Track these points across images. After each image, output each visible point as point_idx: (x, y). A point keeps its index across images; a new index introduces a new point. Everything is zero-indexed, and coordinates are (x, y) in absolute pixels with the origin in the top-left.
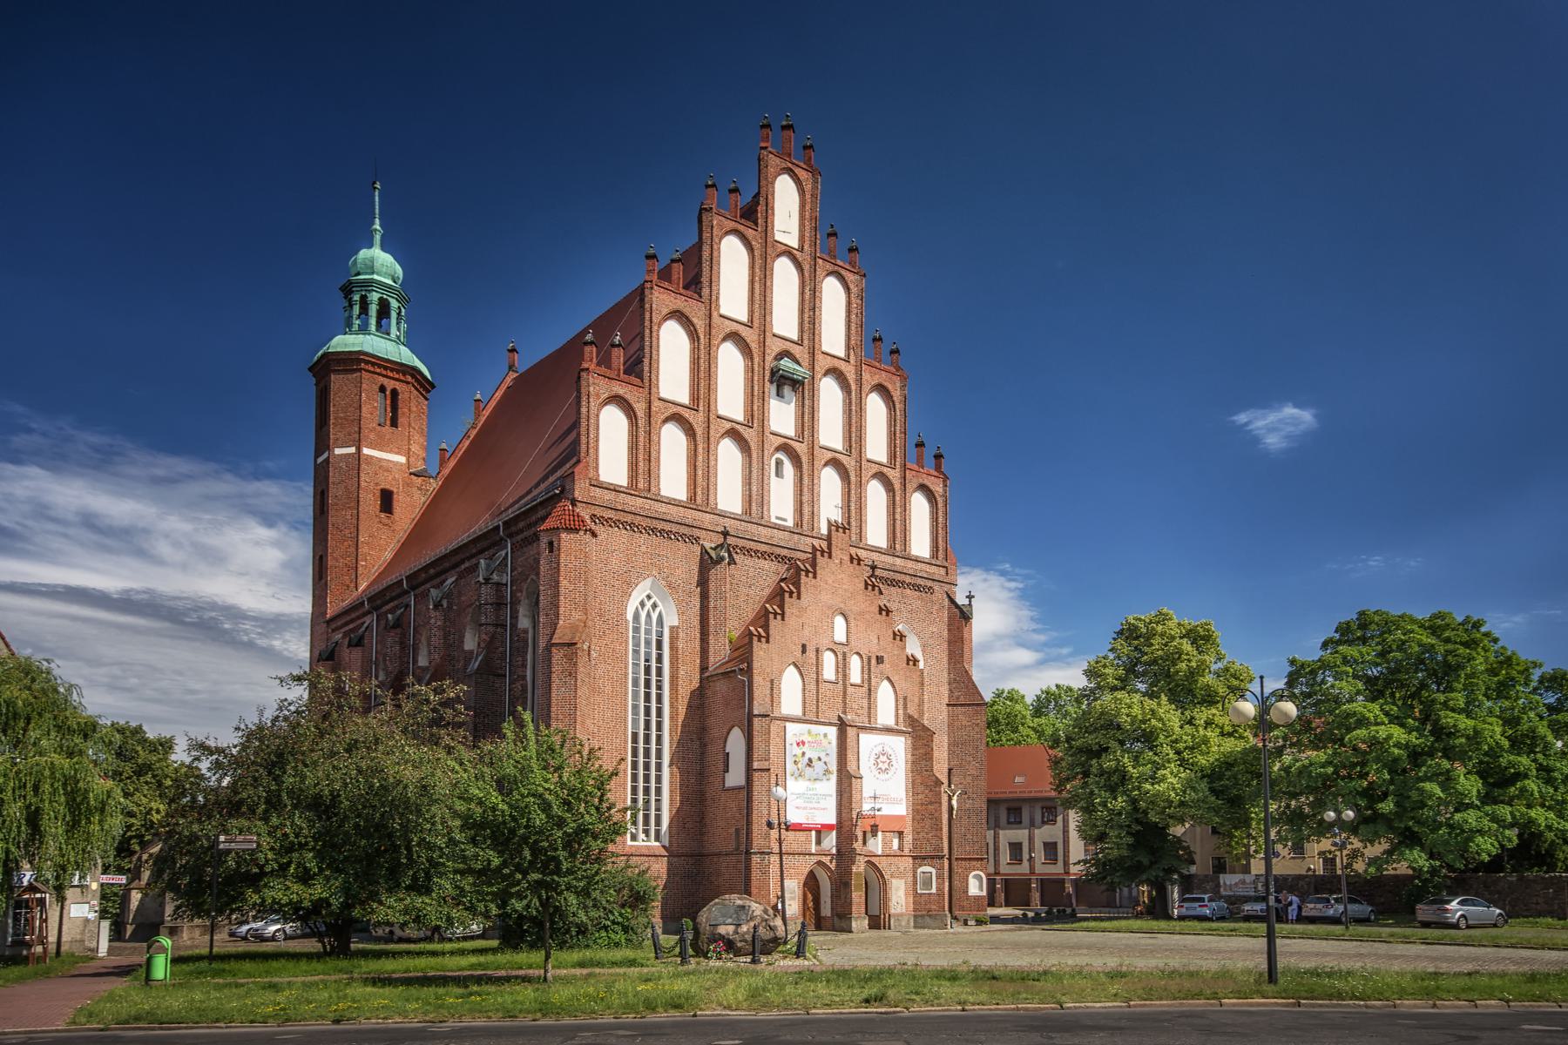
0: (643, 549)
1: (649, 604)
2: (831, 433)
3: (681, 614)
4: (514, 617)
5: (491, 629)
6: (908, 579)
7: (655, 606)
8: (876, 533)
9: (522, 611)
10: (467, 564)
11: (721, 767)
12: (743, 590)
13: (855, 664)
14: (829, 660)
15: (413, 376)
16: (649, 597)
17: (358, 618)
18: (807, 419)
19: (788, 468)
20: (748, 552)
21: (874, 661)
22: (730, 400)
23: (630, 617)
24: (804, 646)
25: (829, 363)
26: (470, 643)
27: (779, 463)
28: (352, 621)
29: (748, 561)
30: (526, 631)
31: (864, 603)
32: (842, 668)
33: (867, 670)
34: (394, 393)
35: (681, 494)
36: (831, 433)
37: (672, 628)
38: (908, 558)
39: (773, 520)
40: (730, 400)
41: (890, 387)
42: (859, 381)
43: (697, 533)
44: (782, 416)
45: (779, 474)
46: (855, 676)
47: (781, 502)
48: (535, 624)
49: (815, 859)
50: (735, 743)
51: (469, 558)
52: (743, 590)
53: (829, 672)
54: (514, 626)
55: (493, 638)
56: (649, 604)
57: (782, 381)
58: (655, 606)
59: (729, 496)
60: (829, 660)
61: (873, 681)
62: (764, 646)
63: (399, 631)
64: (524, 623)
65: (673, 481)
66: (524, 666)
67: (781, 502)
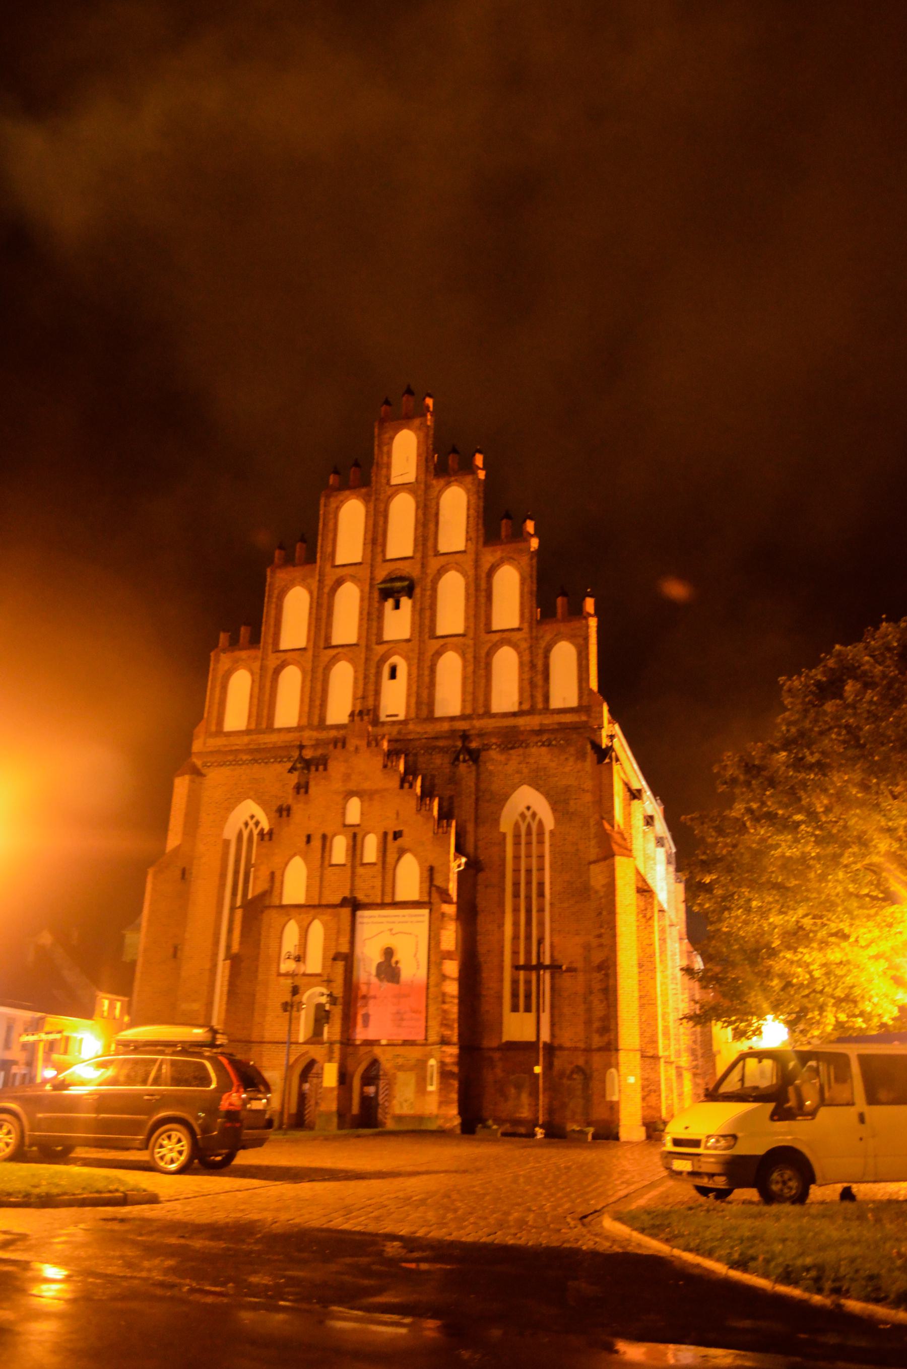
1: (251, 824)
21: (390, 837)
32: (355, 848)
45: (393, 676)
56: (251, 824)
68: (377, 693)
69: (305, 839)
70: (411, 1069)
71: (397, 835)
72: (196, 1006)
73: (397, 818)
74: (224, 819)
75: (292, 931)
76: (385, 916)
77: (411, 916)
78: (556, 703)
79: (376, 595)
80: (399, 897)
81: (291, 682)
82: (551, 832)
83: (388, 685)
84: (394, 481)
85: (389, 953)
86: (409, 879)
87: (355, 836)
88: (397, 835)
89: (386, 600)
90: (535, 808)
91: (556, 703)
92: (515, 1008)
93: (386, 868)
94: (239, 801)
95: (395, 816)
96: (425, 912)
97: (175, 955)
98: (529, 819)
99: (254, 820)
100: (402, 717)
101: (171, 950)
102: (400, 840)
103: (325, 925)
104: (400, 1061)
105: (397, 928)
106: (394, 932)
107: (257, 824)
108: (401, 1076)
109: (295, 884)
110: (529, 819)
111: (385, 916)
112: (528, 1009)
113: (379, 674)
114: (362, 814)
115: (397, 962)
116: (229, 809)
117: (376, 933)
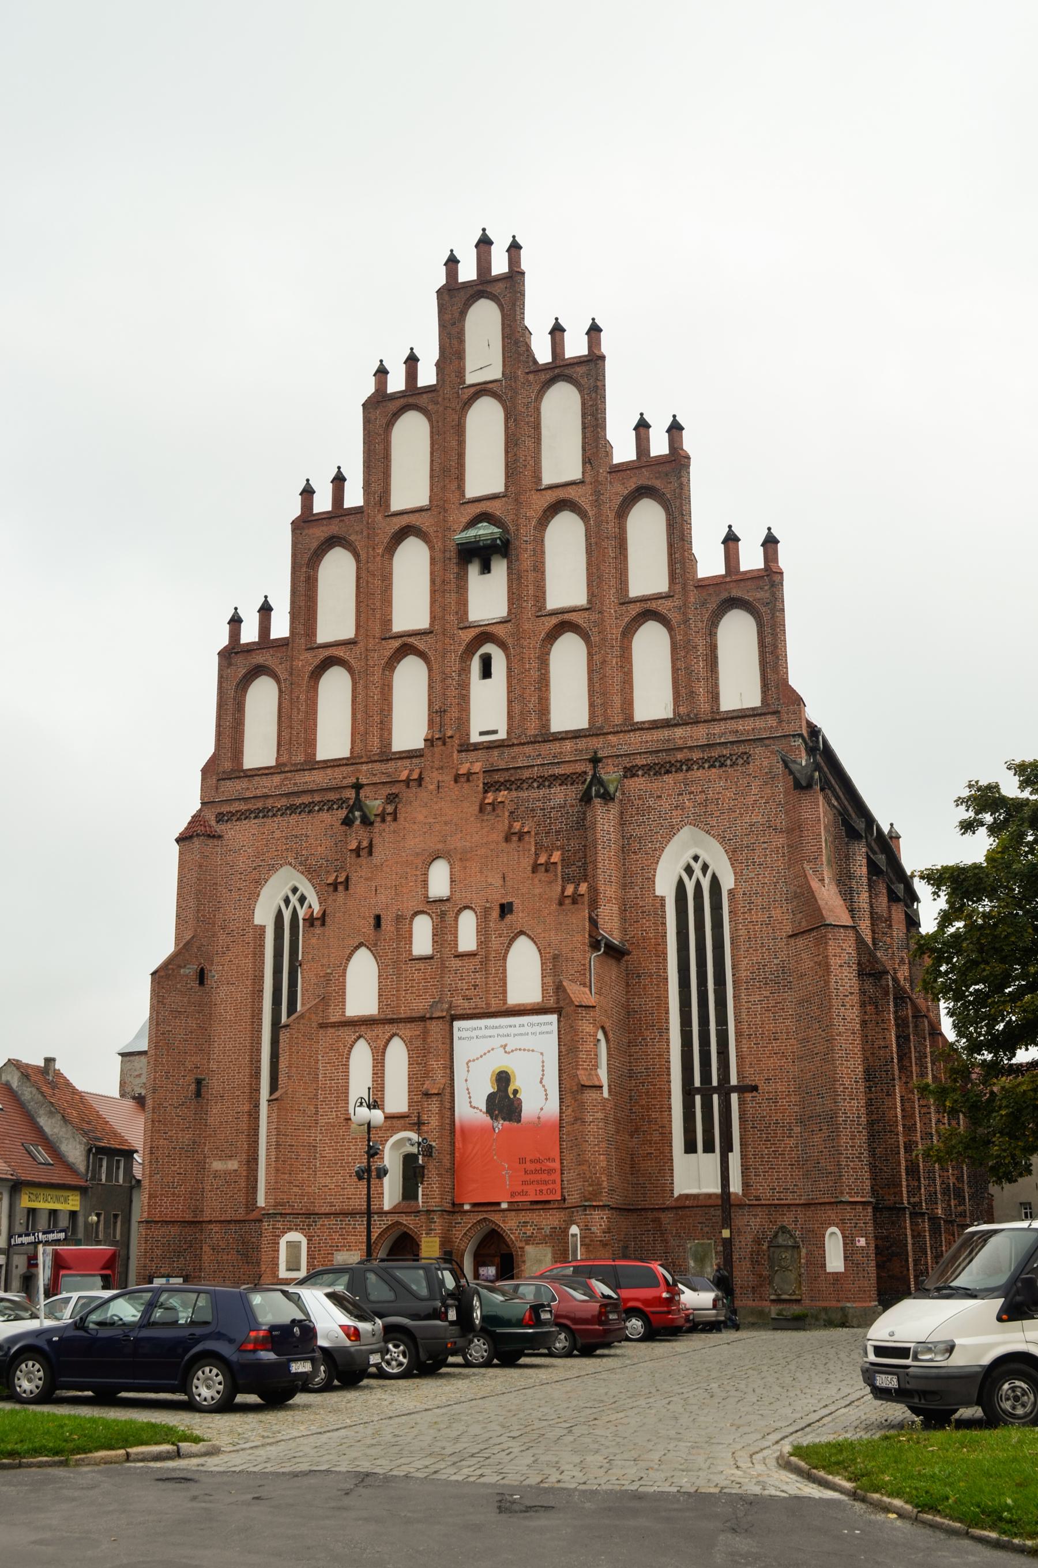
0: (277, 834)
1: (294, 900)
6: (696, 755)
16: (295, 890)
18: (527, 587)
21: (495, 913)
22: (411, 608)
24: (378, 919)
25: (550, 497)
32: (444, 933)
33: (483, 931)
38: (718, 717)
40: (411, 608)
41: (657, 484)
42: (597, 503)
44: (487, 597)
45: (486, 673)
49: (389, 1220)
56: (294, 900)
57: (480, 555)
61: (495, 943)
68: (464, 700)
69: (372, 921)
70: (544, 1241)
71: (505, 909)
72: (233, 1165)
73: (504, 886)
74: (254, 896)
75: (361, 1056)
76: (493, 1027)
77: (532, 1025)
78: (728, 703)
80: (515, 997)
82: (731, 892)
83: (478, 687)
84: (471, 379)
85: (503, 1079)
86: (524, 973)
87: (443, 915)
88: (505, 909)
89: (469, 562)
90: (704, 856)
91: (728, 703)
92: (690, 1147)
93: (490, 960)
94: (273, 869)
95: (501, 882)
96: (553, 1018)
97: (198, 1094)
98: (698, 872)
99: (298, 894)
100: (502, 735)
101: (193, 1087)
102: (509, 918)
103: (409, 1043)
104: (529, 1230)
105: (512, 1043)
106: (508, 1049)
107: (302, 899)
108: (530, 1249)
109: (362, 989)
110: (698, 872)
111: (493, 1027)
112: (709, 1148)
113: (465, 671)
115: (516, 1092)
116: (259, 882)
117: (481, 1052)
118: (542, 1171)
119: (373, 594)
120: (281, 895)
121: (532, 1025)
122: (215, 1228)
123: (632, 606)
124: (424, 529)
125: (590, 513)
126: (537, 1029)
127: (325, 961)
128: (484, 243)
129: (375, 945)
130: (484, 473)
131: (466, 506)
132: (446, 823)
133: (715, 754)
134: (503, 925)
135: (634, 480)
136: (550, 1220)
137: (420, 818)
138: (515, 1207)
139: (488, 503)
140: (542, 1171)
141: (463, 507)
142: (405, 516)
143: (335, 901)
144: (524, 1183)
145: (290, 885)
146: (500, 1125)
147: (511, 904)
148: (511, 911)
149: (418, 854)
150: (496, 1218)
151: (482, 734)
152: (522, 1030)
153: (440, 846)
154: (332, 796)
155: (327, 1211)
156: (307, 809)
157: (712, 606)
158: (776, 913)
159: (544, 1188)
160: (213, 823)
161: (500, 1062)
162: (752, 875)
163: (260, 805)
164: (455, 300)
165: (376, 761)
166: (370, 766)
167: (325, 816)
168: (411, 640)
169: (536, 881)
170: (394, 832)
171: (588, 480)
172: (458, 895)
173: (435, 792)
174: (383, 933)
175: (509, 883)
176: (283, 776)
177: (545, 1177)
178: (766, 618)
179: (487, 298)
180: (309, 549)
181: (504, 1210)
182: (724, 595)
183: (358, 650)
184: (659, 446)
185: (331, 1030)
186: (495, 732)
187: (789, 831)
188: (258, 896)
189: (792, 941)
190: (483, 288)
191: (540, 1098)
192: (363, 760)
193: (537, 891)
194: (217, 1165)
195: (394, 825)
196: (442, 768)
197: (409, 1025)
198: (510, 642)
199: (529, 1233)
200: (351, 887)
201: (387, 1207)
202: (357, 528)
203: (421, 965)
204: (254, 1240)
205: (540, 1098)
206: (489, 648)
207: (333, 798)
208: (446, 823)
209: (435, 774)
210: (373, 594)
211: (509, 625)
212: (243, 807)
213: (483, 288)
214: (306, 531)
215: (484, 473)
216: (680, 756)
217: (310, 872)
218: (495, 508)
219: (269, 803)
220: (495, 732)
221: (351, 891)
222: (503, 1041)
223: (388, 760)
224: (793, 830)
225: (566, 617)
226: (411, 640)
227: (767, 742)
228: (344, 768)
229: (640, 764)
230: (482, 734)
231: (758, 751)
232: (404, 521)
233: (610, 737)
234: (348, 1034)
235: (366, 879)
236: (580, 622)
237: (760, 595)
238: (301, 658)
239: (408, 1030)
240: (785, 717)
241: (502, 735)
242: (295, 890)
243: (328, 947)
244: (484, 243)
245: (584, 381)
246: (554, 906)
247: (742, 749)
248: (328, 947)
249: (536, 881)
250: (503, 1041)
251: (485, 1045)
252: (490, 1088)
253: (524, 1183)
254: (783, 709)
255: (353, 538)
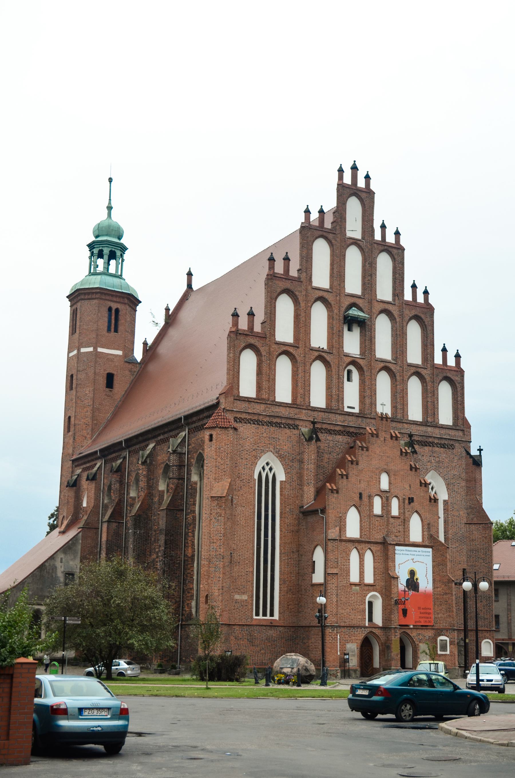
0: (265, 435)
1: (267, 468)
2: (383, 350)
3: (286, 473)
4: (189, 474)
5: (176, 481)
6: (436, 441)
7: (271, 469)
8: (415, 412)
9: (193, 470)
10: (162, 437)
11: (310, 570)
12: (326, 456)
13: (395, 504)
14: (377, 502)
15: (128, 299)
16: (268, 464)
17: (93, 460)
19: (355, 375)
20: (330, 432)
21: (407, 501)
22: (319, 338)
23: (256, 477)
24: (361, 494)
25: (382, 306)
26: (162, 487)
27: (349, 372)
28: (89, 462)
29: (330, 438)
30: (196, 483)
31: (401, 465)
32: (386, 506)
34: (117, 311)
35: (288, 399)
36: (383, 350)
37: (281, 482)
39: (346, 409)
40: (319, 338)
41: (423, 316)
42: (402, 315)
43: (297, 422)
44: (351, 343)
45: (349, 380)
46: (395, 511)
47: (351, 397)
48: (201, 477)
49: (368, 630)
50: (319, 556)
51: (164, 433)
52: (326, 456)
53: (377, 509)
54: (189, 479)
55: (177, 487)
56: (267, 468)
57: (351, 322)
58: (271, 469)
59: (318, 398)
60: (377, 502)
61: (407, 515)
62: (335, 495)
63: (119, 474)
64: (195, 478)
65: (283, 393)
66: (195, 504)
67: (351, 397)
71: (411, 500)
72: (245, 597)
75: (354, 556)
77: (423, 552)
79: (342, 318)
81: (284, 368)
83: (347, 385)
85: (412, 573)
88: (411, 500)
94: (263, 452)
96: (430, 550)
100: (357, 410)
105: (416, 558)
106: (414, 561)
114: (390, 483)
115: (417, 579)
116: (257, 458)
118: (426, 613)
119: (302, 323)
120: (262, 466)
121: (423, 552)
122: (237, 628)
123: (412, 368)
124: (329, 301)
125: (398, 320)
126: (424, 554)
127: (339, 510)
128: (354, 168)
129: (360, 506)
130: (353, 285)
131: (348, 297)
132: (388, 457)
133: (443, 442)
134: (410, 507)
135: (414, 311)
136: (429, 633)
137: (378, 452)
138: (416, 627)
139: (357, 299)
140: (426, 613)
141: (346, 297)
142: (321, 291)
143: (342, 483)
144: (420, 617)
145: (266, 462)
146: (411, 592)
147: (413, 498)
148: (413, 501)
149: (377, 468)
150: (408, 631)
151: (348, 407)
152: (419, 553)
153: (386, 467)
154: (291, 422)
155: (343, 625)
156: (278, 425)
157: (441, 378)
158: (461, 513)
159: (427, 620)
160: (233, 421)
161: (411, 566)
162: (454, 496)
163: (256, 418)
164: (345, 191)
165: (309, 410)
166: (306, 411)
167: (287, 431)
168: (323, 354)
169: (422, 490)
170: (367, 456)
171: (397, 304)
172: (392, 491)
173: (383, 442)
174: (362, 503)
175: (412, 489)
176: (266, 405)
177: (427, 616)
178: (459, 389)
179: (357, 197)
180: (276, 291)
181: (411, 629)
182: (445, 375)
183: (301, 350)
184: (420, 299)
185: (344, 543)
186: (354, 408)
187: (467, 481)
188: (256, 464)
189: (468, 525)
190: (354, 191)
191: (426, 583)
192: (304, 408)
193: (422, 494)
194: (237, 597)
195: (367, 453)
196: (386, 431)
197: (375, 545)
198: (365, 369)
199: (420, 638)
200: (349, 477)
201: (367, 625)
202: (299, 289)
203: (379, 519)
204: (256, 634)
205: (426, 583)
206: (351, 367)
207: (290, 423)
208: (388, 457)
209: (383, 433)
210: (302, 323)
211: (365, 360)
212: (248, 417)
213: (354, 191)
214: (274, 281)
215: (353, 285)
216: (431, 440)
217: (281, 458)
218: (360, 302)
219: (261, 418)
220: (354, 408)
221: (350, 480)
222: (413, 557)
223: (314, 410)
224: (470, 481)
225: (387, 364)
226: (323, 354)
227: (460, 442)
228: (294, 409)
229: (416, 439)
230: (348, 407)
231: (457, 445)
232: (321, 294)
233: (405, 424)
234: (349, 545)
235: (356, 475)
236: (393, 368)
237: (457, 378)
238: (273, 347)
239: (374, 548)
240: (466, 433)
241: (357, 410)
242: (268, 464)
243: (340, 504)
244: (354, 168)
245: (396, 257)
246: (428, 502)
247: (451, 442)
248: (340, 504)
249: (422, 490)
250: (413, 557)
251: (406, 558)
252: (407, 577)
253: (420, 617)
254: (466, 430)
255: (297, 293)
